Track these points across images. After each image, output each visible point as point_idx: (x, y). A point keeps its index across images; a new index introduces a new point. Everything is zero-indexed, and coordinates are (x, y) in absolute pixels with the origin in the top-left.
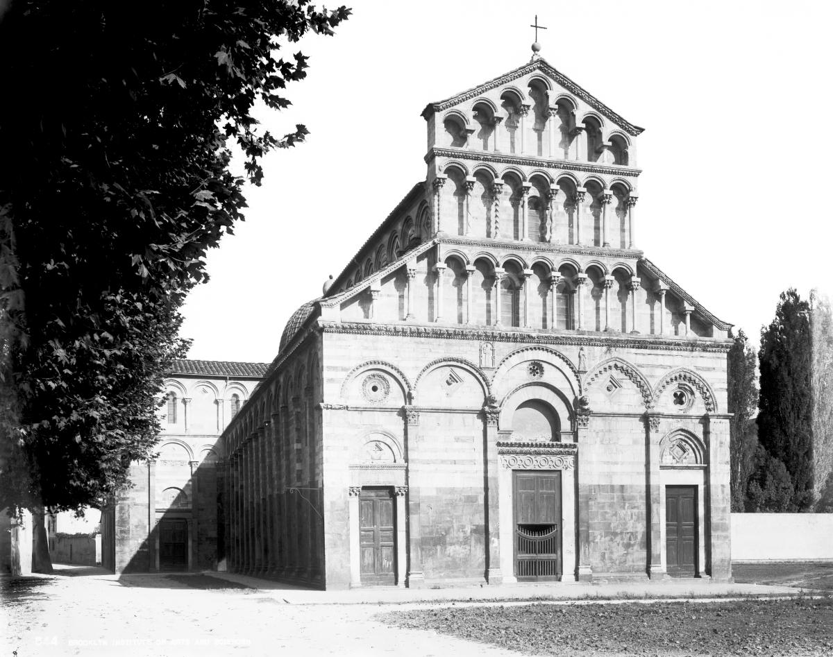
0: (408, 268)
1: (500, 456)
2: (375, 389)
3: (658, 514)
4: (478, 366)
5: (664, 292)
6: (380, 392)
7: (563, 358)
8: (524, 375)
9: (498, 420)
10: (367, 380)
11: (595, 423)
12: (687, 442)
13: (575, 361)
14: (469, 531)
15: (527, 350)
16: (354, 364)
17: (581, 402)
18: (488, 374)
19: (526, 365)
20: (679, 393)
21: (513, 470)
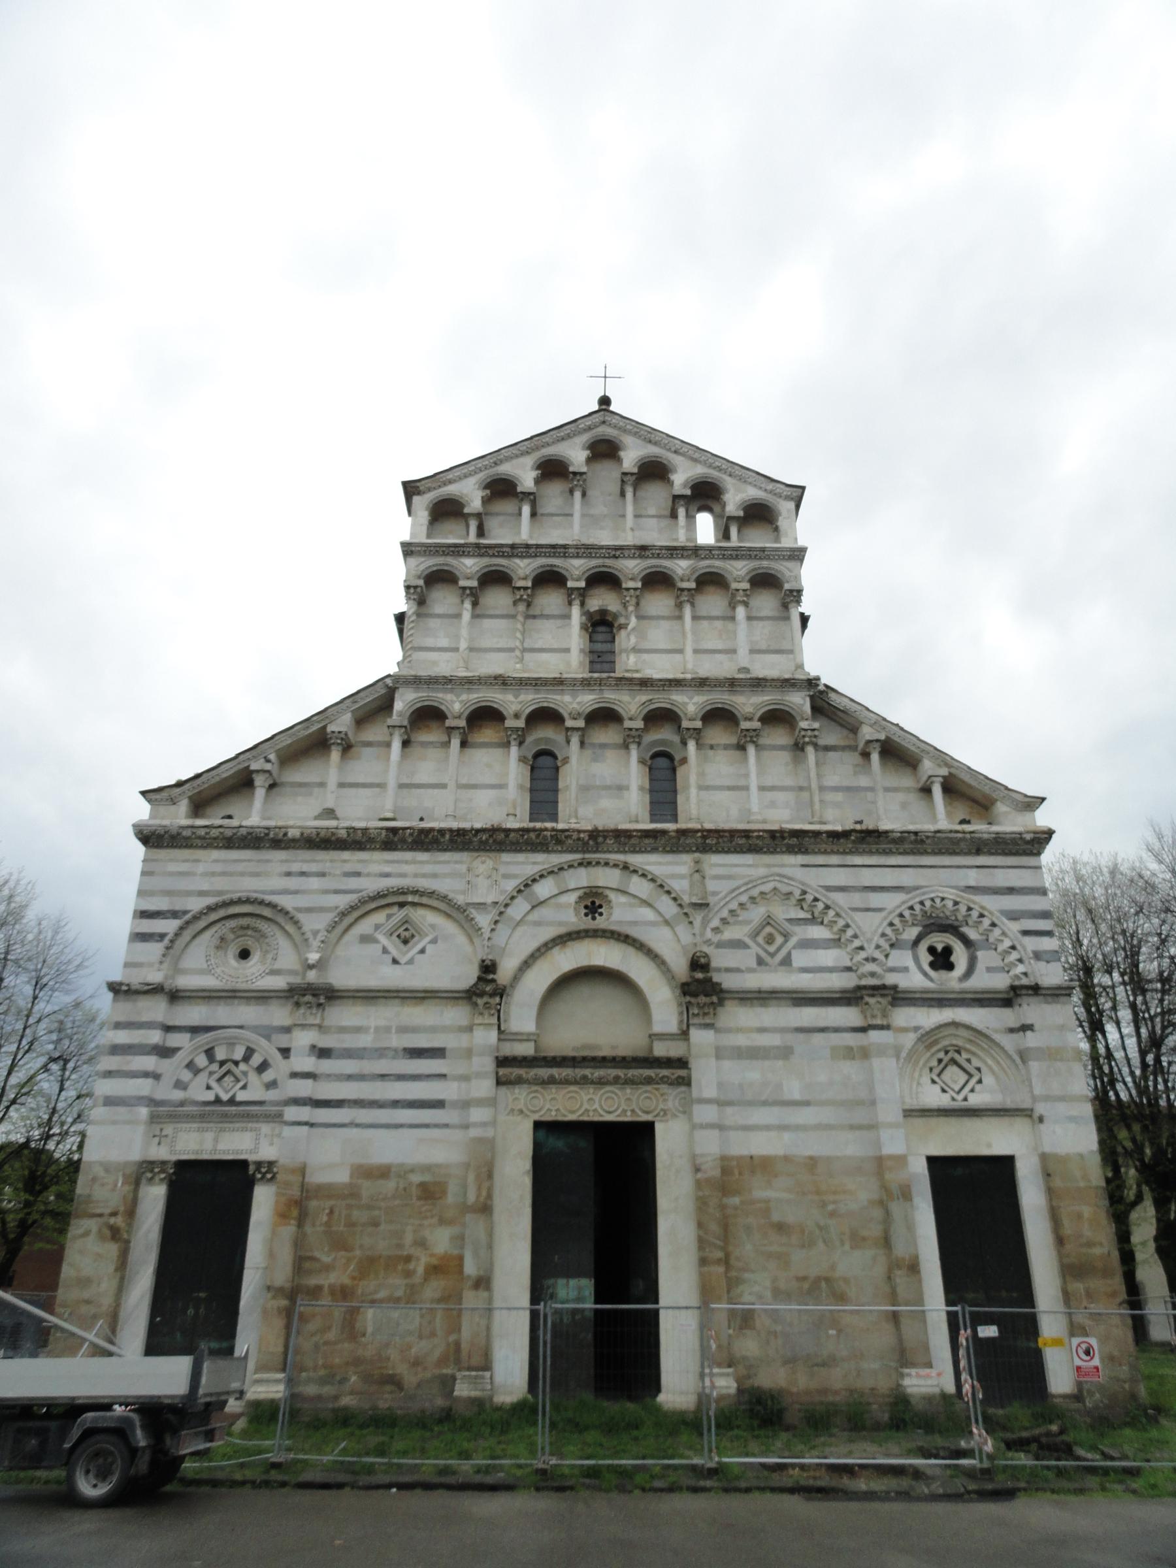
0: (330, 729)
1: (503, 1090)
2: (244, 954)
3: (910, 1227)
4: (460, 899)
5: (877, 745)
6: (255, 958)
7: (653, 880)
8: (570, 917)
9: (499, 1011)
10: (232, 936)
11: (736, 1016)
12: (974, 1054)
13: (680, 886)
14: (420, 1270)
15: (571, 866)
16: (196, 905)
17: (698, 964)
18: (484, 920)
19: (572, 898)
20: (939, 947)
21: (538, 1125)
